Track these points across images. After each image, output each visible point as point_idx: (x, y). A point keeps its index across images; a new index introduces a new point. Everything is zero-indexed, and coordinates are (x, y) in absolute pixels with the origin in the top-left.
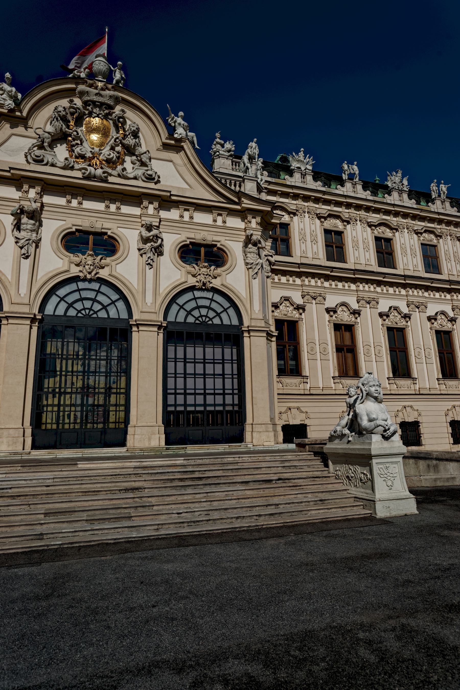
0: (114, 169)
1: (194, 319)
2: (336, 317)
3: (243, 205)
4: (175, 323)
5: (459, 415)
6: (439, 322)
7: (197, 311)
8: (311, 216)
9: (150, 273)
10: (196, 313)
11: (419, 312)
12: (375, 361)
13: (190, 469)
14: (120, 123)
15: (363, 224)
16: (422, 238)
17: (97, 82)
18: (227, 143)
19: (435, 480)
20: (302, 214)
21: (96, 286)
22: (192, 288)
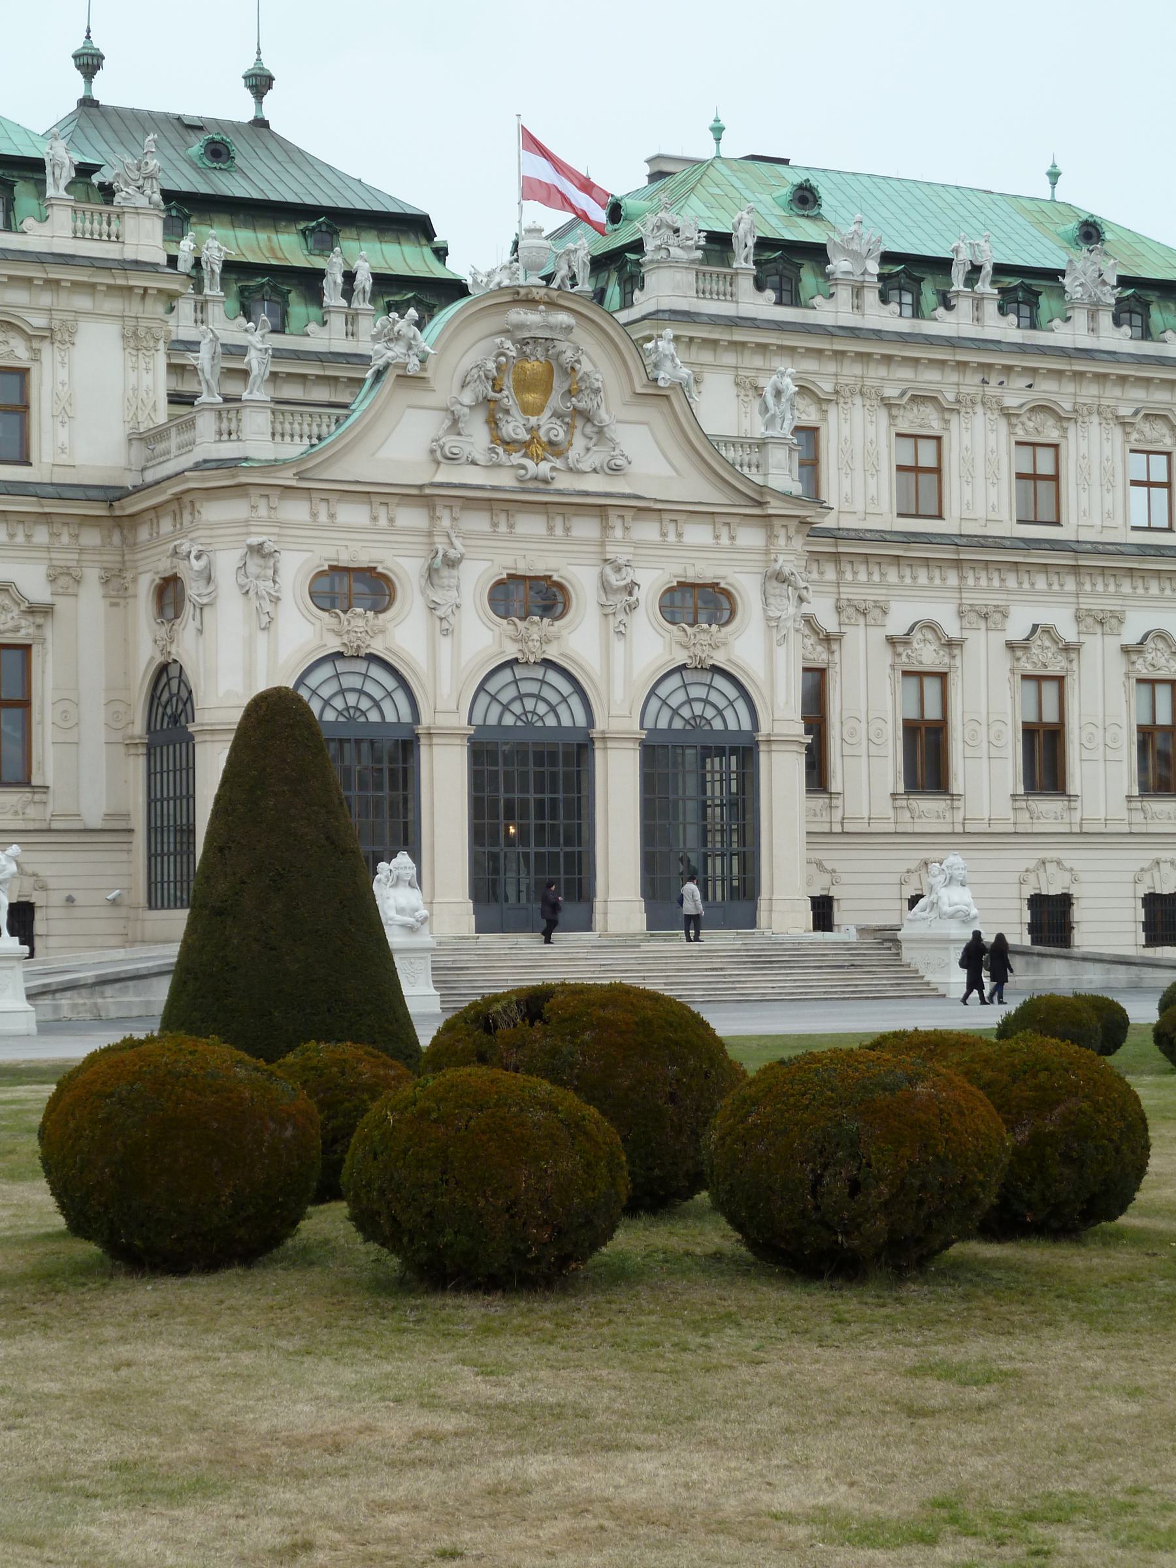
0: (558, 455)
2: (908, 656)
4: (653, 731)
5: (1172, 883)
6: (1149, 656)
7: (687, 707)
8: (868, 403)
9: (618, 647)
10: (686, 712)
11: (1103, 634)
12: (987, 764)
14: (570, 371)
15: (989, 413)
16: (1135, 436)
19: (1034, 981)
20: (849, 401)
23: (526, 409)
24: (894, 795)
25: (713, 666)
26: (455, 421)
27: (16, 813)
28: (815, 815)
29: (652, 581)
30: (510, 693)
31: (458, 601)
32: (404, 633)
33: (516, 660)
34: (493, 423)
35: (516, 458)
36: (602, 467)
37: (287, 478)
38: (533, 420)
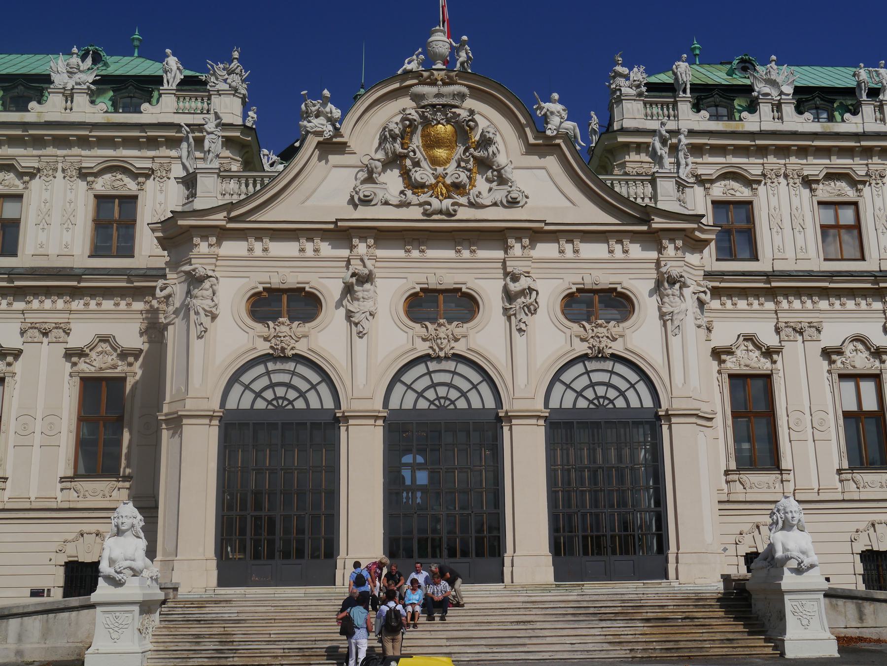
0: (463, 194)
1: (588, 403)
2: (843, 363)
3: (654, 226)
13: (585, 604)
17: (435, 72)
18: (635, 69)
20: (775, 180)
21: (451, 365)
22: (583, 358)
23: (435, 162)
24: (839, 472)
25: (613, 355)
26: (371, 172)
27: (104, 496)
28: (769, 487)
29: (550, 291)
30: (425, 382)
31: (372, 309)
32: (325, 338)
33: (428, 355)
34: (405, 174)
35: (423, 198)
36: (501, 202)
37: (219, 219)
38: (440, 170)
